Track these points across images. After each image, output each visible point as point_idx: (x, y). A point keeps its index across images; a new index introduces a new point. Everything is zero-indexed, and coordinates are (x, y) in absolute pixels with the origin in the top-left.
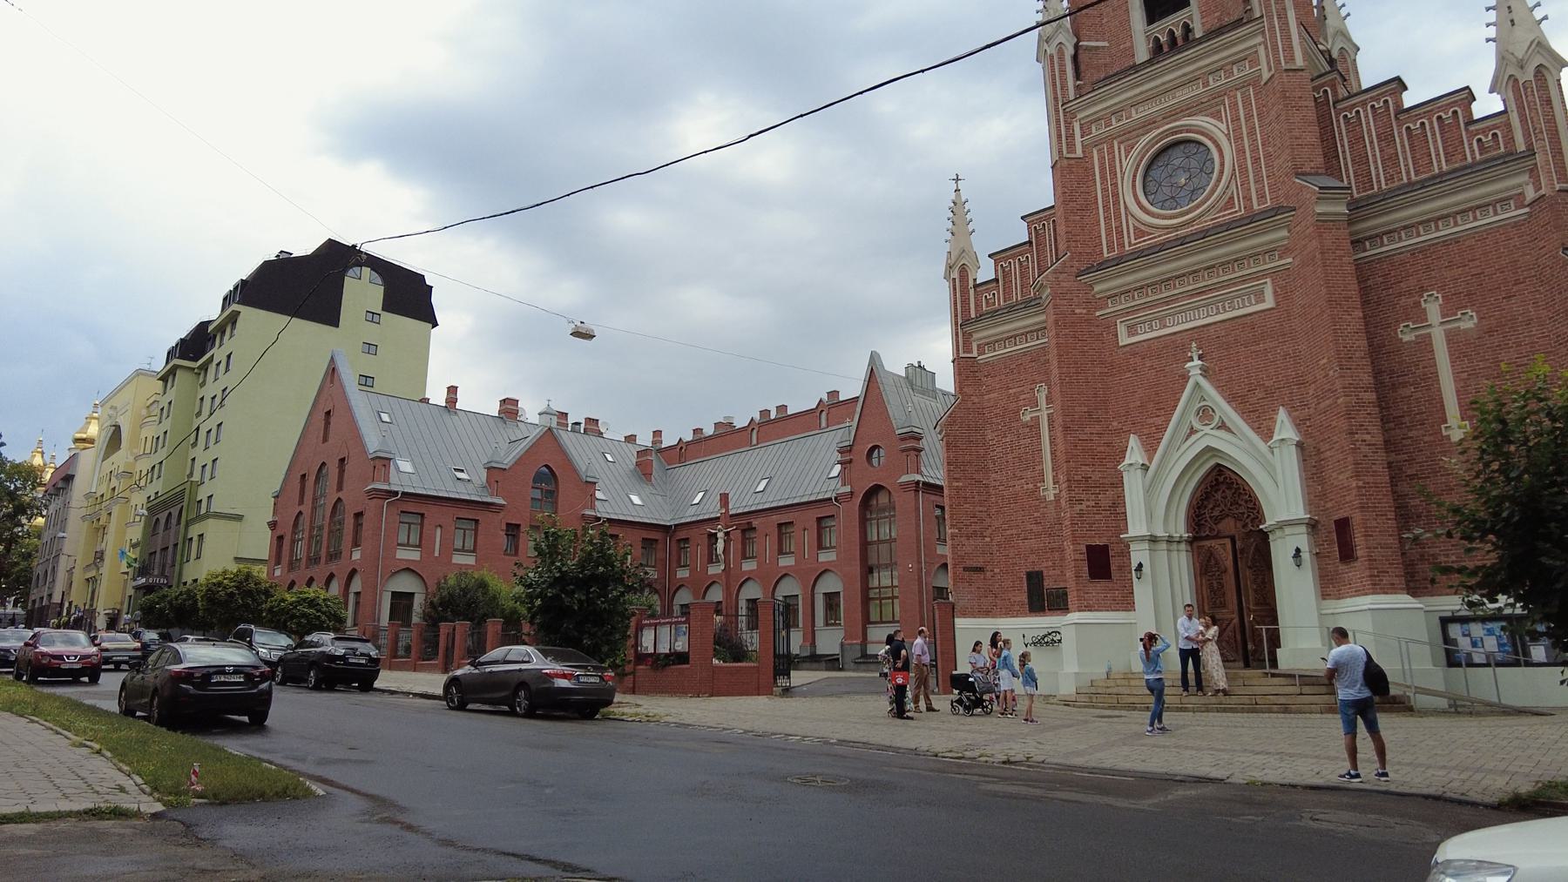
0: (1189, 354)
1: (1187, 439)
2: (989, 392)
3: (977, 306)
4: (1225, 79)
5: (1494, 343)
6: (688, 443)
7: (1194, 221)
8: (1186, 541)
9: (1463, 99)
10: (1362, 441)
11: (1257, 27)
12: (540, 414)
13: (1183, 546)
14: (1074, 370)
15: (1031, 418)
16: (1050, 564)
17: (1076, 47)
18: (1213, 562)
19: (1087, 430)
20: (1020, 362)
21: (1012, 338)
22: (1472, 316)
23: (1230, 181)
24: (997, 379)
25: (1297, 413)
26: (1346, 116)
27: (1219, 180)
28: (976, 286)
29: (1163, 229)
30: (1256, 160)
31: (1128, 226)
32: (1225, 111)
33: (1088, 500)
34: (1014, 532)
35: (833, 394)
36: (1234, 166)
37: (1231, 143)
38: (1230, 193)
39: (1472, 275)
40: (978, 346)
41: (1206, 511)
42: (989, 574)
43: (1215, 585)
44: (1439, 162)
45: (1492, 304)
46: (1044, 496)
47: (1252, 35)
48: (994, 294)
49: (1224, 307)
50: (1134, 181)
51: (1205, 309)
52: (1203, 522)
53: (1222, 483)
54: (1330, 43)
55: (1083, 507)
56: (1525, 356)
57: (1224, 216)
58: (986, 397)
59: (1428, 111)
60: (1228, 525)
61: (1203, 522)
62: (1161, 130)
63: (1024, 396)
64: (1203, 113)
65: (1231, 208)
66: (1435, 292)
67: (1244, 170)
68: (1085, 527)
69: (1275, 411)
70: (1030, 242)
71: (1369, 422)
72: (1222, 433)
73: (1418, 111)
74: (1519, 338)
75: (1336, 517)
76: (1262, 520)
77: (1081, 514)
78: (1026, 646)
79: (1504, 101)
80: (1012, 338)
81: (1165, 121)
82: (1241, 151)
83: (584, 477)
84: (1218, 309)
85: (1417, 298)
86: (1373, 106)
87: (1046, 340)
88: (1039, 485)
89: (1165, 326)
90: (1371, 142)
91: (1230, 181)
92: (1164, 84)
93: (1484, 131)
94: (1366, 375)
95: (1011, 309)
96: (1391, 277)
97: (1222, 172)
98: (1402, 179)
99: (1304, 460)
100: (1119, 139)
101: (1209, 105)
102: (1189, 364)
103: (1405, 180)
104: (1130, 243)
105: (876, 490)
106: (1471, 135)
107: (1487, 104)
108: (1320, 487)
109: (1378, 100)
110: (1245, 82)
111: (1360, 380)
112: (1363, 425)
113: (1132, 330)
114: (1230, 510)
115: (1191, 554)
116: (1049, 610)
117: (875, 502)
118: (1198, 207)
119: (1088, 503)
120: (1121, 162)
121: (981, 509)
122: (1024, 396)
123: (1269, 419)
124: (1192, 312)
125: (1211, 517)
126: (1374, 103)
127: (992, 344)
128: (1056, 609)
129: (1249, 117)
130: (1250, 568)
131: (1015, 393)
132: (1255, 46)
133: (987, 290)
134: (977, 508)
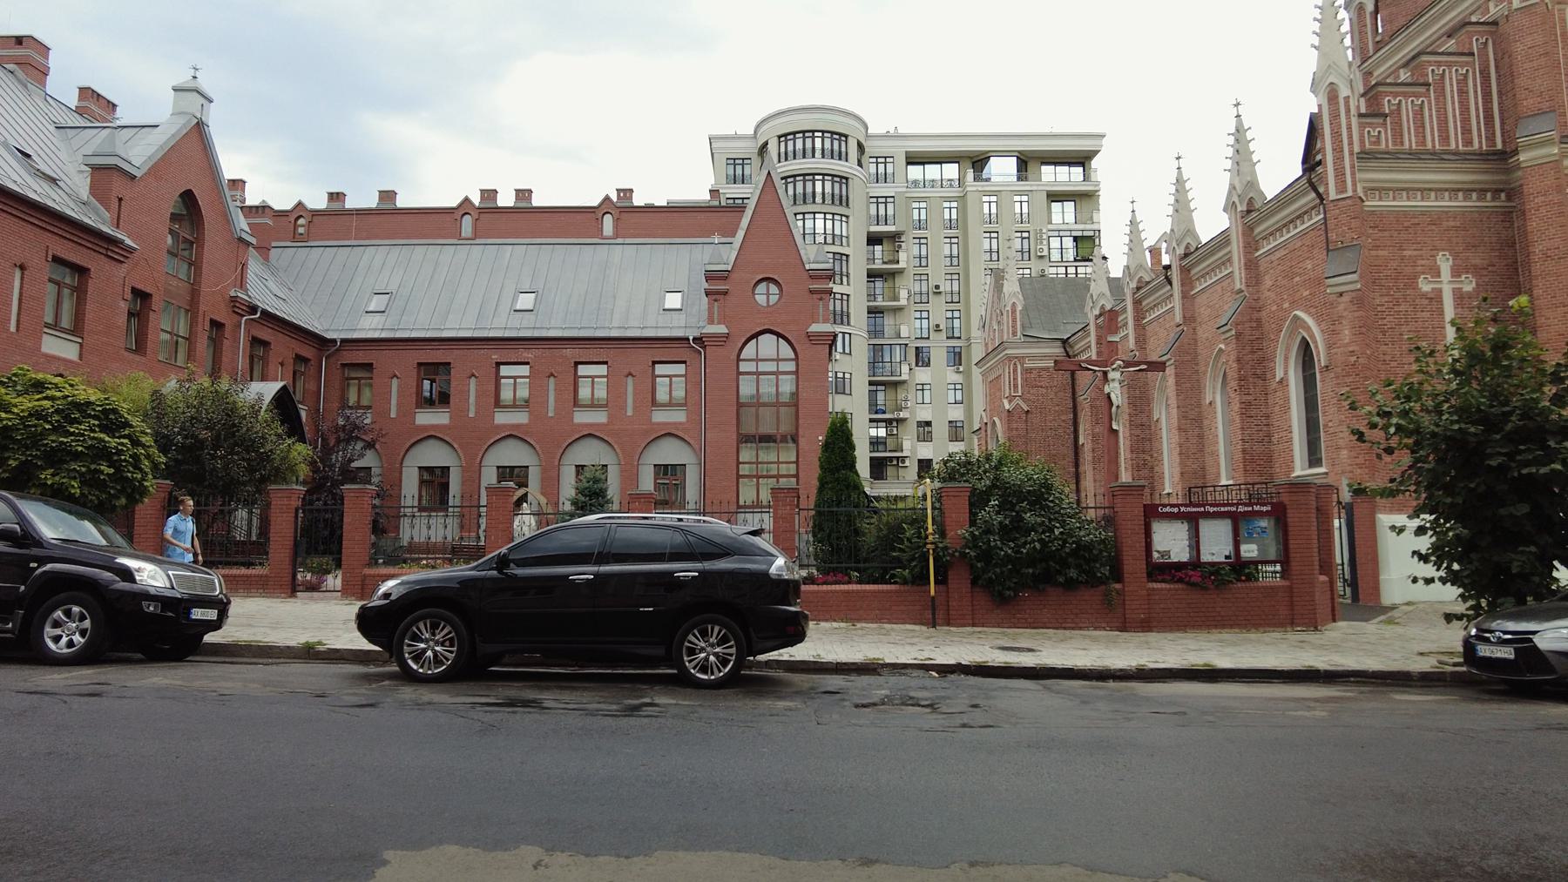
2: (1377, 247)
3: (1362, 142)
6: (316, 213)
12: (176, 90)
15: (1433, 289)
20: (1416, 221)
21: (1410, 190)
24: (1386, 234)
35: (626, 193)
48: (1379, 132)
58: (1374, 253)
63: (1423, 262)
80: (1410, 190)
83: (238, 230)
95: (1418, 156)
103: (1429, 146)
122: (1423, 262)
131: (1410, 256)
133: (1370, 124)
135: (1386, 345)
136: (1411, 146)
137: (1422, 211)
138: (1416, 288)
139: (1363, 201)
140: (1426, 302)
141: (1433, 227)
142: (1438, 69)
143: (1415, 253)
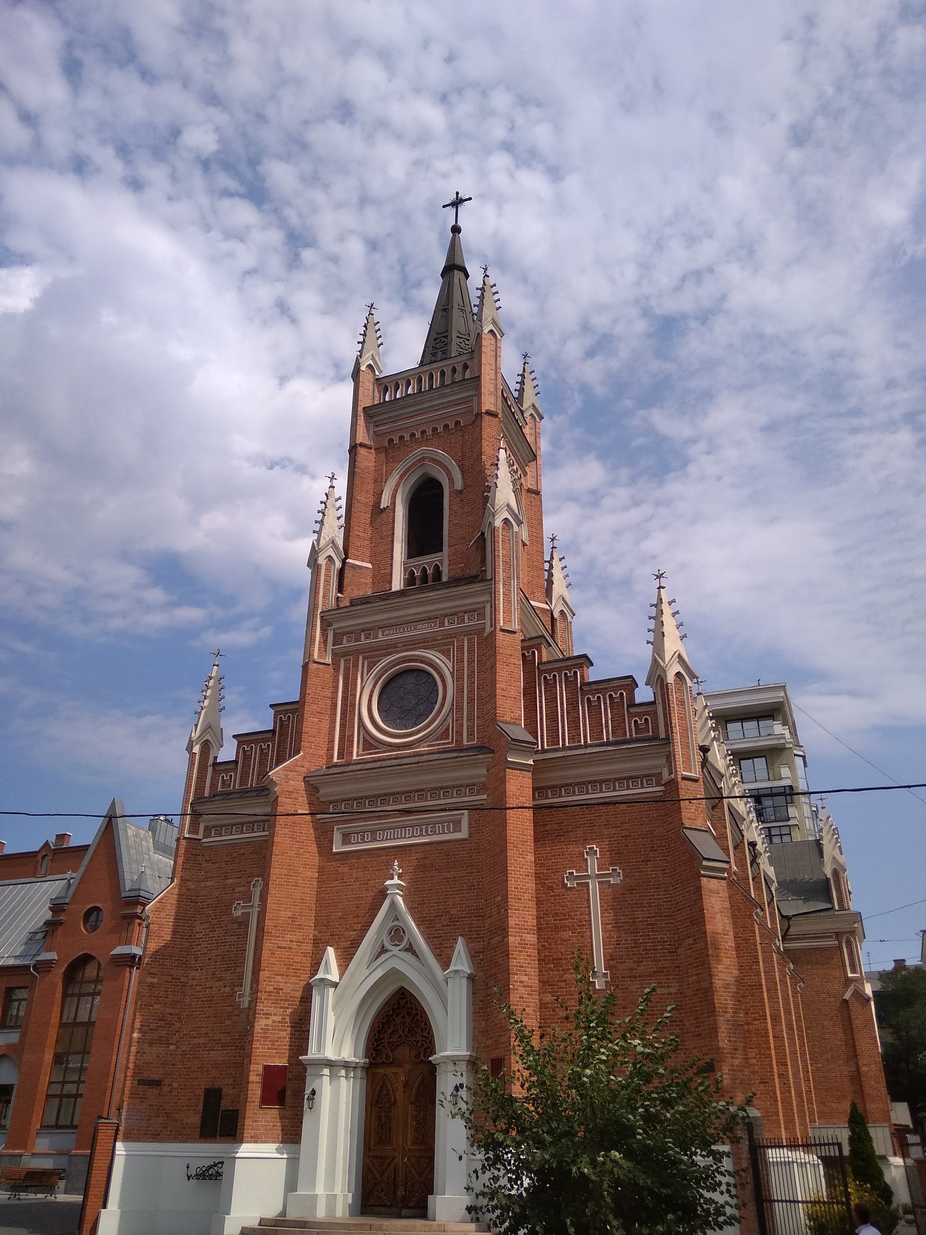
0: (391, 872)
1: (377, 958)
2: (207, 879)
3: (213, 785)
4: (458, 624)
5: (633, 900)
7: (413, 745)
8: (362, 1067)
9: (627, 685)
10: (520, 982)
11: (484, 588)
13: (359, 1073)
14: (286, 872)
15: (242, 913)
16: (232, 1080)
17: (344, 562)
18: (384, 1093)
19: (289, 937)
20: (242, 851)
22: (619, 873)
23: (448, 714)
25: (473, 945)
26: (547, 677)
27: (440, 711)
28: (215, 764)
29: (387, 746)
30: (471, 701)
31: (358, 736)
32: (454, 651)
33: (275, 1015)
34: (202, 1040)
36: (453, 702)
37: (453, 681)
38: (447, 724)
39: (622, 837)
40: (206, 828)
41: (385, 1035)
42: (166, 1089)
43: (383, 1119)
44: (607, 732)
45: (633, 865)
46: (240, 1002)
47: (481, 593)
48: (231, 776)
49: (427, 831)
50: (371, 696)
51: (411, 829)
52: (380, 1048)
53: (404, 1007)
54: (553, 604)
55: (269, 1022)
56: (653, 917)
57: (439, 745)
58: (203, 884)
59: (605, 689)
60: (403, 1052)
61: (380, 1048)
62: (400, 655)
64: (436, 649)
65: (445, 739)
66: (595, 846)
67: (460, 708)
68: (267, 1045)
69: (455, 940)
70: (273, 731)
71: (529, 964)
72: (408, 956)
73: (594, 687)
74: (650, 899)
75: (492, 1056)
76: (433, 1052)
77: (265, 1031)
78: (189, 1179)
79: (654, 693)
81: (404, 648)
82: (460, 690)
84: (421, 831)
85: (582, 849)
86: (566, 674)
87: (267, 833)
88: (236, 989)
89: (374, 840)
90: (562, 704)
91: (448, 714)
92: (408, 615)
93: (640, 715)
94: (530, 917)
96: (564, 826)
97: (443, 705)
98: (580, 741)
99: (474, 993)
100: (364, 655)
101: (442, 644)
102: (388, 882)
104: (358, 752)
105: (86, 959)
106: (631, 715)
107: (644, 694)
108: (484, 1023)
109: (570, 671)
110: (473, 630)
111: (525, 921)
112: (523, 967)
113: (346, 840)
114: (406, 1036)
115: (365, 1081)
116: (221, 1136)
117: (80, 975)
118: (419, 732)
119: (275, 1018)
120: (362, 676)
121: (172, 1011)
122: (240, 889)
123: (450, 947)
124: (399, 830)
125: (388, 1043)
126: (567, 672)
127: (219, 829)
128: (227, 1135)
129: (471, 662)
130: (412, 1103)
132: (483, 602)
133: (226, 771)
134: (169, 1010)
135: (196, 970)
136: (252, 785)
137: (248, 842)
138: (230, 914)
139: (200, 840)
140: (236, 926)
141: (255, 855)
142: (285, 716)
143: (237, 881)
